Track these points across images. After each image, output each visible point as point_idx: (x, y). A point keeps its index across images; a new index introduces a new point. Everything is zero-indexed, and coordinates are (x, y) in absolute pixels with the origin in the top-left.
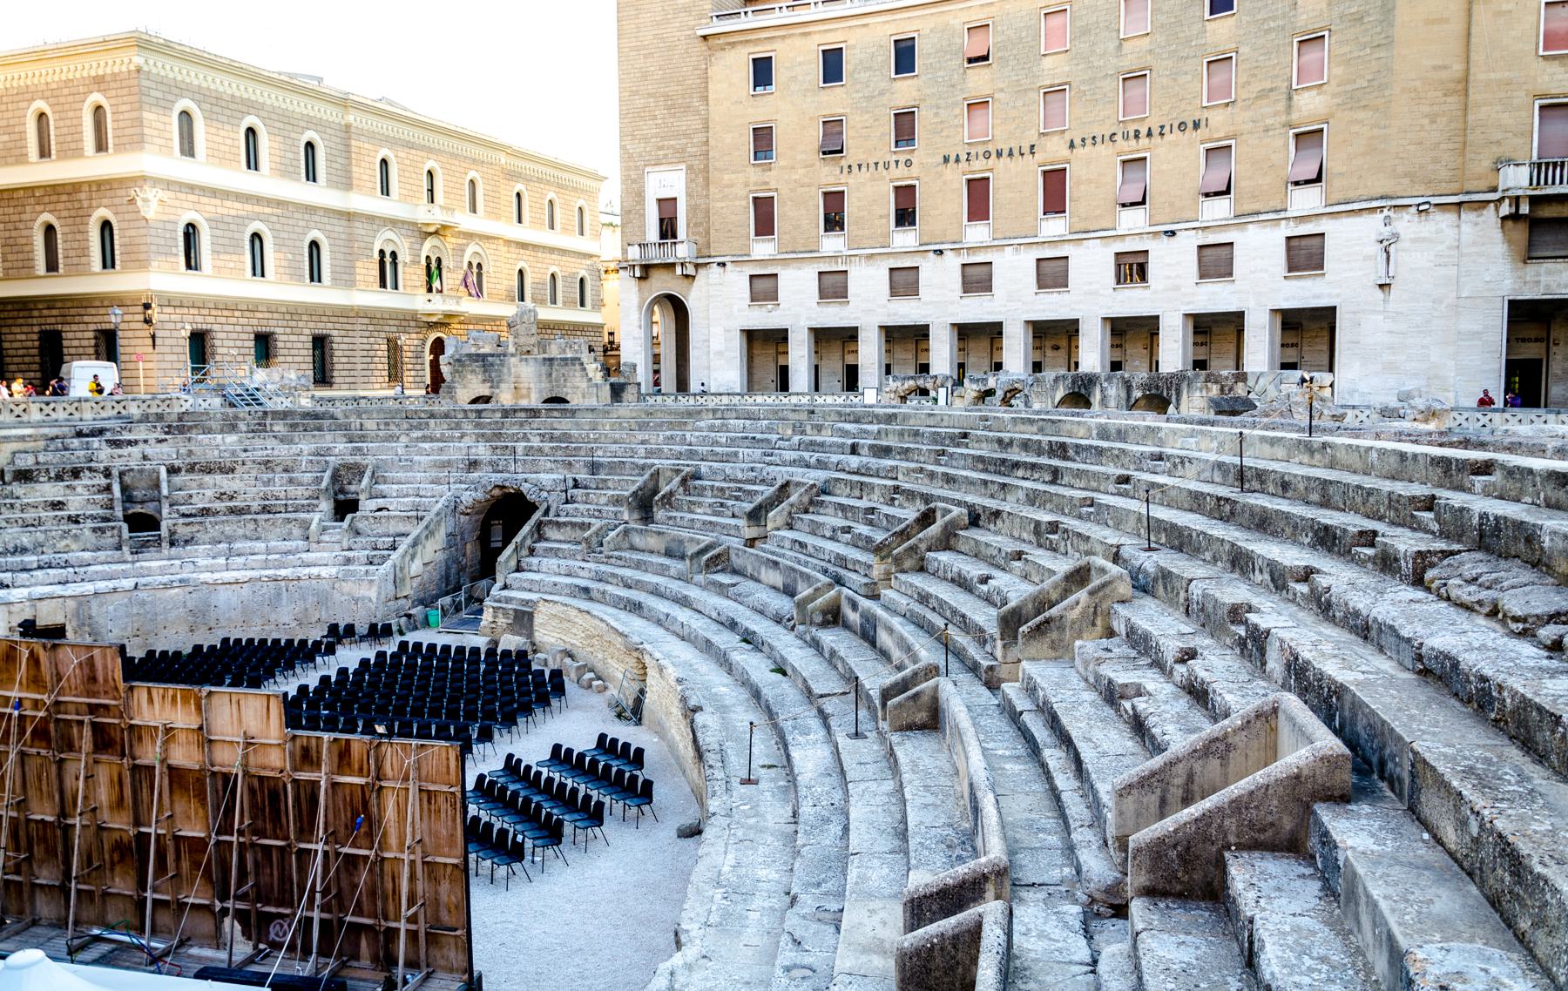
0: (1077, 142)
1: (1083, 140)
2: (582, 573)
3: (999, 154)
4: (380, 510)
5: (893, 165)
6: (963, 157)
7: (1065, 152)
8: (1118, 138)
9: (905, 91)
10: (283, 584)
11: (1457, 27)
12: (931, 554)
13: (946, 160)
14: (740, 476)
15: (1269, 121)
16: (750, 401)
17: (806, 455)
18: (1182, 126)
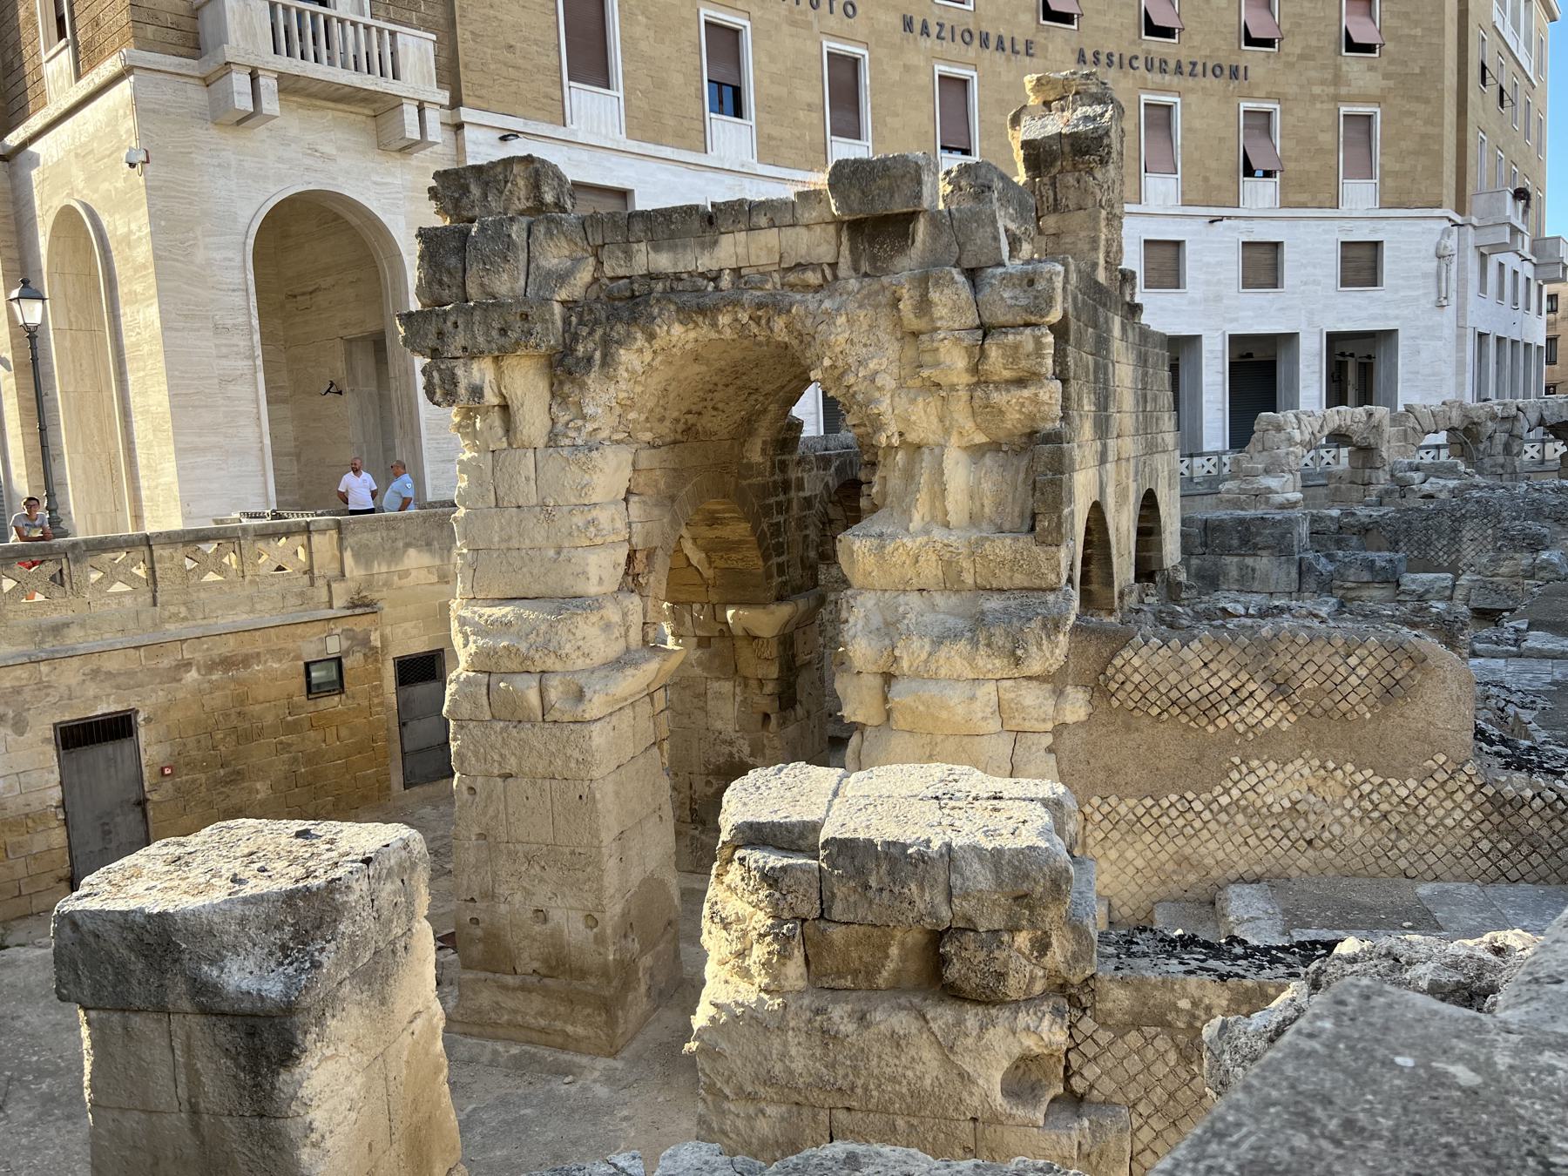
0: (1089, 56)
1: (1096, 54)
3: (984, 42)
8: (1140, 63)
13: (908, 24)
15: (1317, 90)
18: (1217, 70)
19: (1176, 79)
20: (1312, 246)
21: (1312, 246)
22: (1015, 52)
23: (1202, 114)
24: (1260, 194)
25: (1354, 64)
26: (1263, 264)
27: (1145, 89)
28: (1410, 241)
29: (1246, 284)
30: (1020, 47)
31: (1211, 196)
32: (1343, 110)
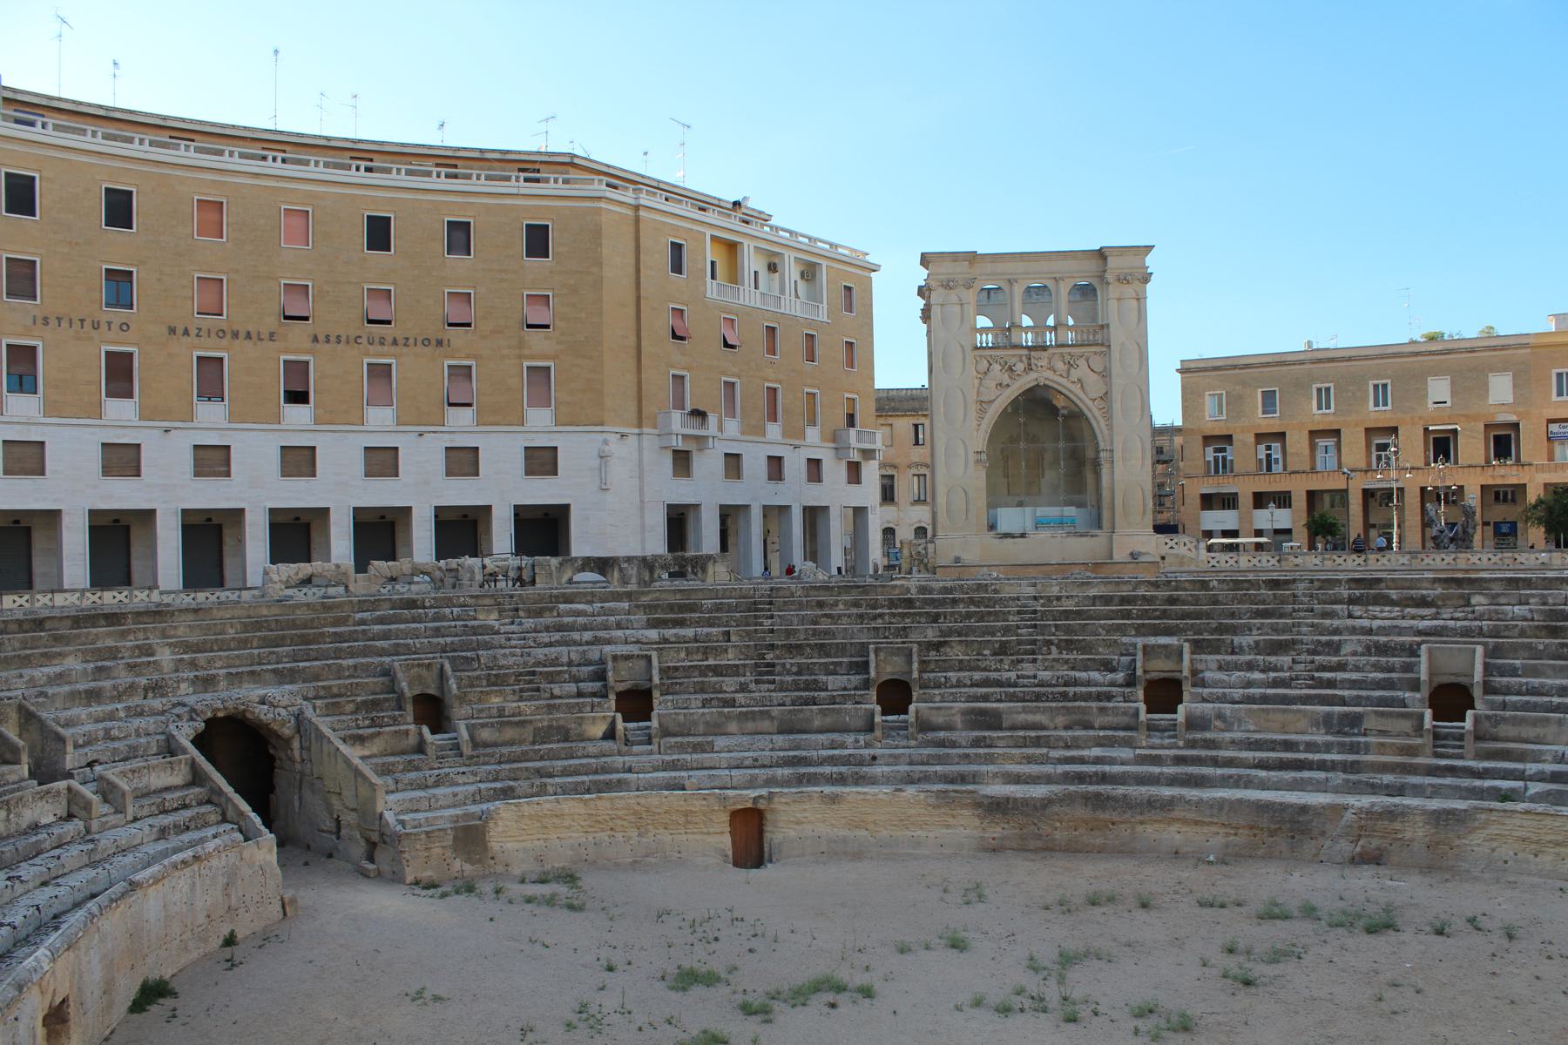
0: (321, 337)
1: (327, 337)
2: (461, 779)
4: (90, 765)
5: (104, 327)
6: (193, 332)
7: (308, 345)
8: (364, 341)
9: (118, 248)
10: (196, 867)
11: (632, 311)
12: (925, 676)
13: (172, 331)
14: (503, 662)
15: (505, 352)
16: (188, 599)
17: (576, 636)
18: (426, 342)
19: (393, 348)
20: (502, 454)
21: (502, 454)
22: (260, 339)
23: (416, 371)
24: (462, 418)
25: (535, 337)
26: (463, 461)
27: (368, 355)
28: (575, 448)
29: (450, 473)
30: (265, 336)
31: (419, 417)
32: (526, 364)
